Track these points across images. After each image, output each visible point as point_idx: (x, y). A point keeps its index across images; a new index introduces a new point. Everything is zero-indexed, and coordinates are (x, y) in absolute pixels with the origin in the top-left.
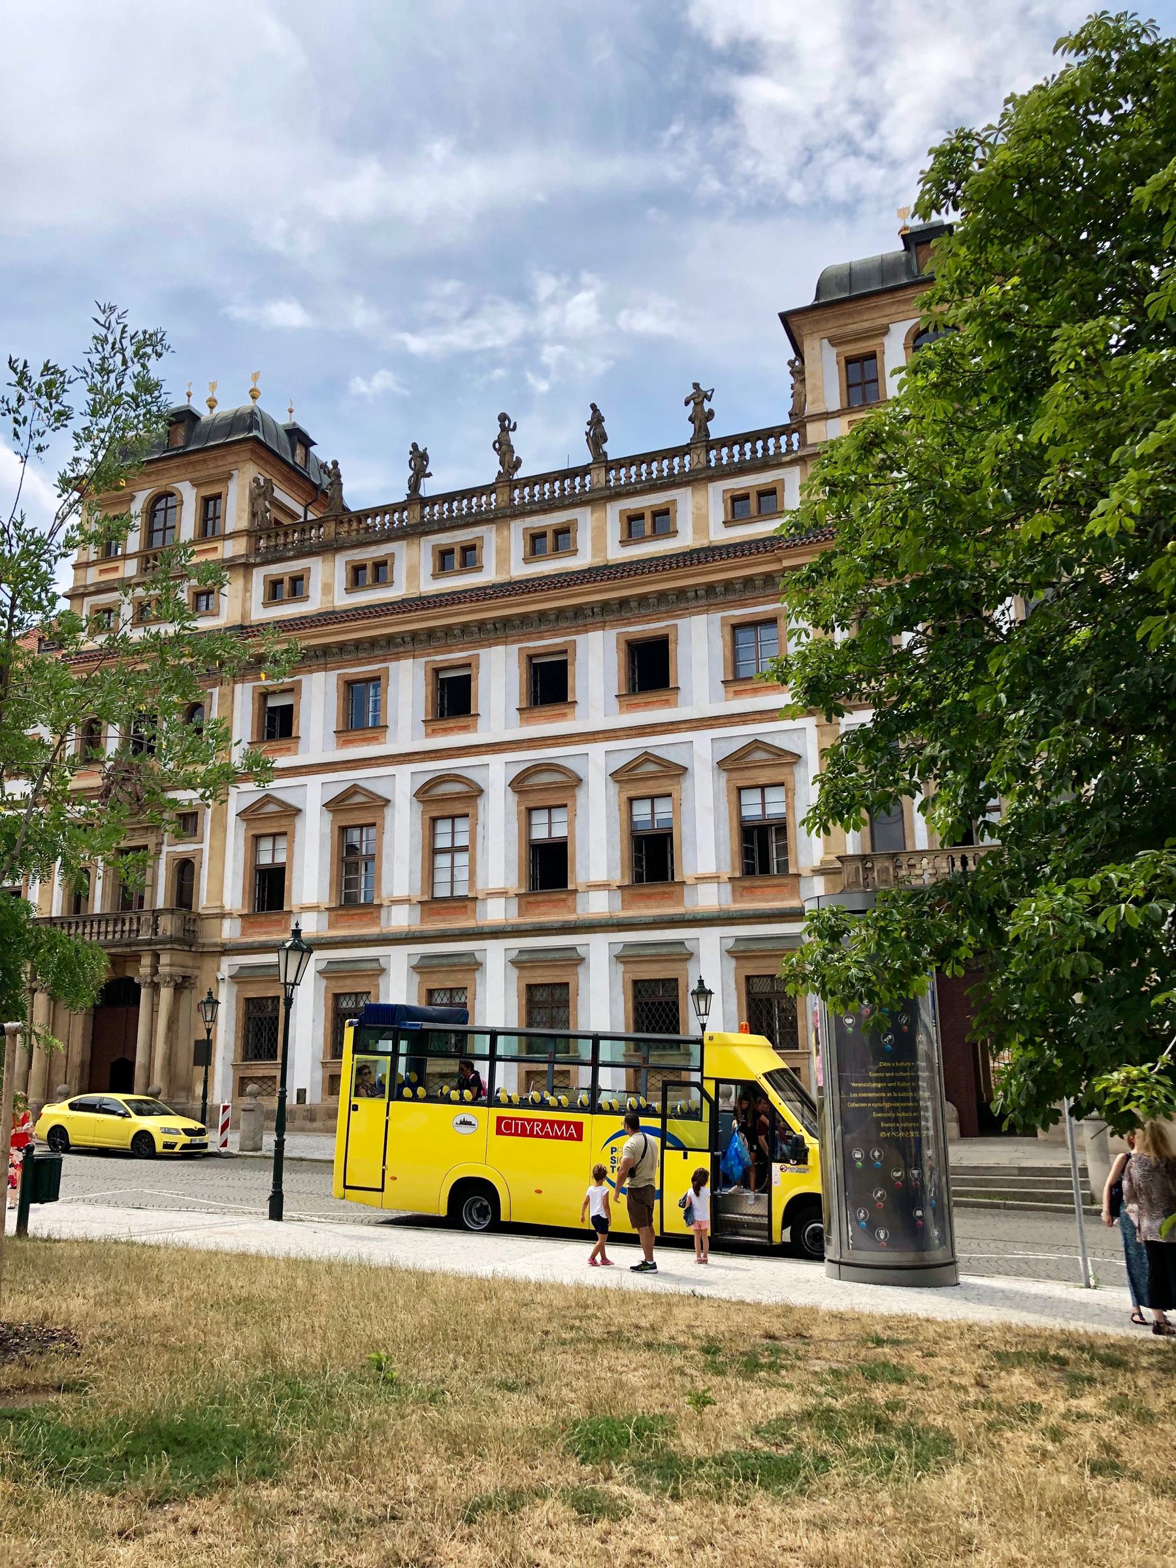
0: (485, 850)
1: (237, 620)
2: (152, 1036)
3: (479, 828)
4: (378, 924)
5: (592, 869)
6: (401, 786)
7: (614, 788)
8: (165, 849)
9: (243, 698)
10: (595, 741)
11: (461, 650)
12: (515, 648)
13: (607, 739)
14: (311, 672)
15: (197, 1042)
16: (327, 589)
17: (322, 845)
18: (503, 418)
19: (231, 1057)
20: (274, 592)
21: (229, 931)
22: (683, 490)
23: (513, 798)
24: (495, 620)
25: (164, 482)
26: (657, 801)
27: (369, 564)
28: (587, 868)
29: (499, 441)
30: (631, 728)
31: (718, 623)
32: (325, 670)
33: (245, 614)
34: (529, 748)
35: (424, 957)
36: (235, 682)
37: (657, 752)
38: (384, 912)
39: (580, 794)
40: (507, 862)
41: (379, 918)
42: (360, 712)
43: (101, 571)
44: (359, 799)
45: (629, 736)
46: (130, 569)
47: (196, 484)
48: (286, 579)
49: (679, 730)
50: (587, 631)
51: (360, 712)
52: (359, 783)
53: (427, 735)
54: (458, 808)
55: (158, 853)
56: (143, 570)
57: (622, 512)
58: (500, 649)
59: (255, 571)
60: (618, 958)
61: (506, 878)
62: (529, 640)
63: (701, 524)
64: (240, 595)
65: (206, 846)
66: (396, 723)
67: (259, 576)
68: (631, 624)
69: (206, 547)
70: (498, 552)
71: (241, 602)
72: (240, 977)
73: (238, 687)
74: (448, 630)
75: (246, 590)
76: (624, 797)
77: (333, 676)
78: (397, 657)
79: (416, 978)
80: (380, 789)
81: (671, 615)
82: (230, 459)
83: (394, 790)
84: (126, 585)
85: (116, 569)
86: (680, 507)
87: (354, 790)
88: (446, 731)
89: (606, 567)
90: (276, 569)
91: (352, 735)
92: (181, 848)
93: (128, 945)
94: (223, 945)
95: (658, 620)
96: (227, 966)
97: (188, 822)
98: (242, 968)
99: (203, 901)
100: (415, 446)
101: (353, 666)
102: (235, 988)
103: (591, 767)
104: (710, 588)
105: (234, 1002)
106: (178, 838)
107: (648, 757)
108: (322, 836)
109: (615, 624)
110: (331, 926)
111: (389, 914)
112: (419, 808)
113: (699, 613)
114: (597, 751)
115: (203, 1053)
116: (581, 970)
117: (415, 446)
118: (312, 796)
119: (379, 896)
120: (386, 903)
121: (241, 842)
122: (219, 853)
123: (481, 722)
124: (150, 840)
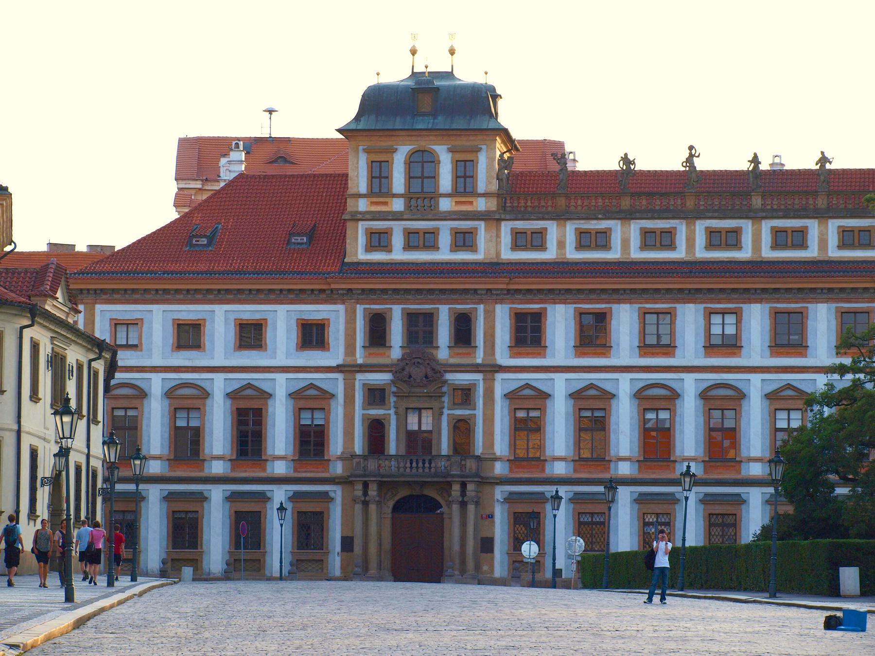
0: (682, 432)
1: (492, 257)
2: (456, 532)
3: (677, 419)
4: (609, 472)
5: (752, 449)
6: (624, 387)
7: (766, 403)
8: (446, 412)
9: (502, 315)
10: (755, 372)
11: (663, 303)
12: (701, 307)
13: (763, 372)
14: (555, 303)
15: (482, 538)
16: (561, 245)
17: (567, 419)
18: (691, 148)
19: (506, 548)
20: (520, 240)
21: (499, 469)
22: (812, 220)
23: (701, 403)
24: (690, 290)
25: (423, 143)
26: (791, 412)
27: (593, 232)
28: (749, 449)
29: (687, 160)
30: (778, 367)
31: (833, 310)
32: (565, 303)
33: (498, 254)
34: (711, 372)
35: (641, 494)
36: (496, 303)
37: (794, 384)
38: (612, 465)
39: (744, 403)
40: (697, 442)
41: (609, 468)
42: (593, 335)
43: (372, 203)
44: (592, 392)
45: (777, 372)
46: (398, 205)
47: (450, 150)
48: (529, 233)
49: (808, 372)
50: (750, 303)
51: (593, 335)
52: (594, 382)
53: (641, 356)
54: (663, 404)
55: (441, 414)
56: (408, 206)
57: (772, 228)
58: (691, 306)
59: (503, 223)
60: (768, 502)
61: (696, 450)
62: (711, 303)
63: (823, 244)
64: (495, 239)
65: (479, 412)
66: (618, 345)
67: (506, 228)
68: (778, 302)
69: (463, 199)
70: (688, 239)
71: (496, 244)
72: (510, 499)
73: (498, 308)
74: (657, 291)
75: (498, 236)
76: (773, 408)
77: (571, 308)
78: (619, 302)
79: (636, 506)
80: (608, 387)
81: (804, 300)
82: (480, 137)
83: (618, 389)
84: (396, 217)
85: (386, 203)
86: (810, 231)
87: (591, 386)
88: (653, 355)
89: (761, 262)
90: (520, 225)
91: (587, 350)
92: (459, 412)
93: (444, 477)
94: (497, 478)
95: (797, 302)
96: (500, 492)
97: (465, 395)
98: (511, 493)
99: (479, 449)
100: (626, 155)
101: (585, 303)
102: (506, 506)
103: (752, 389)
104: (831, 290)
105: (506, 514)
106: (455, 405)
107: (789, 386)
108: (567, 413)
109: (768, 301)
110: (575, 471)
111: (616, 468)
112: (637, 402)
113: (822, 302)
114: (756, 379)
115: (487, 545)
116: (743, 507)
117: (626, 155)
118: (560, 387)
119: (609, 455)
120: (614, 459)
121: (506, 412)
122: (489, 420)
123: (678, 352)
124: (435, 404)
